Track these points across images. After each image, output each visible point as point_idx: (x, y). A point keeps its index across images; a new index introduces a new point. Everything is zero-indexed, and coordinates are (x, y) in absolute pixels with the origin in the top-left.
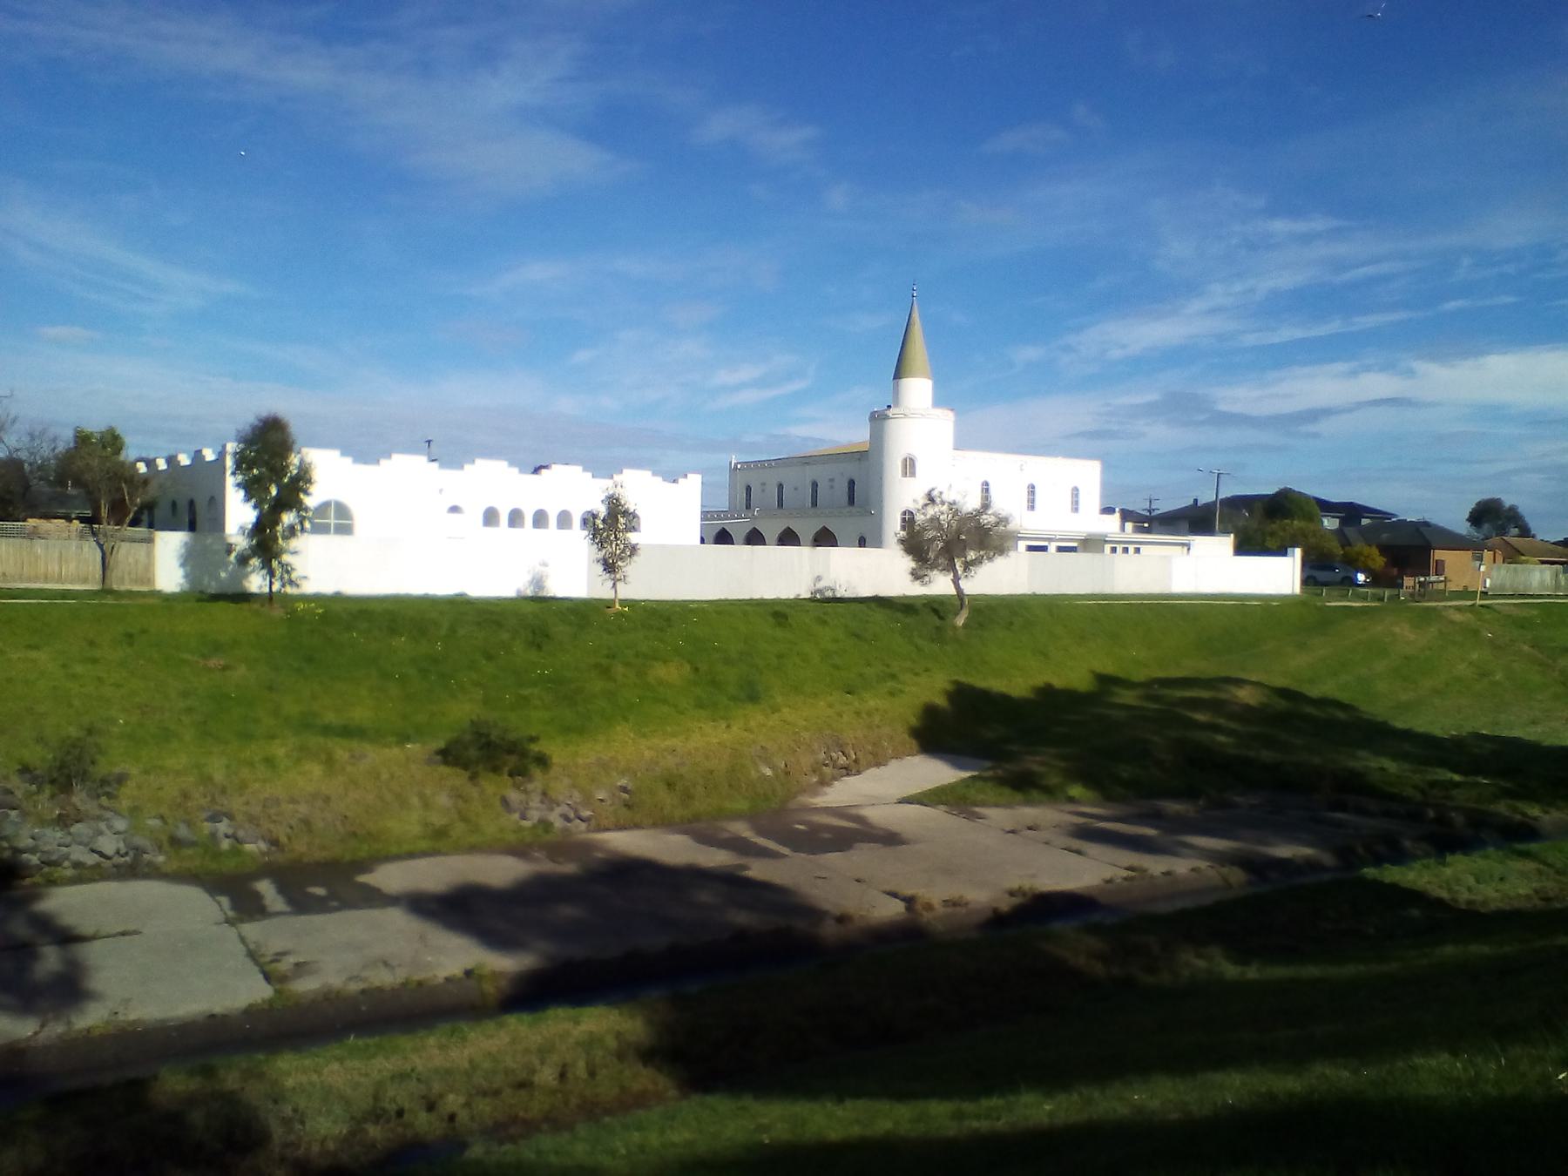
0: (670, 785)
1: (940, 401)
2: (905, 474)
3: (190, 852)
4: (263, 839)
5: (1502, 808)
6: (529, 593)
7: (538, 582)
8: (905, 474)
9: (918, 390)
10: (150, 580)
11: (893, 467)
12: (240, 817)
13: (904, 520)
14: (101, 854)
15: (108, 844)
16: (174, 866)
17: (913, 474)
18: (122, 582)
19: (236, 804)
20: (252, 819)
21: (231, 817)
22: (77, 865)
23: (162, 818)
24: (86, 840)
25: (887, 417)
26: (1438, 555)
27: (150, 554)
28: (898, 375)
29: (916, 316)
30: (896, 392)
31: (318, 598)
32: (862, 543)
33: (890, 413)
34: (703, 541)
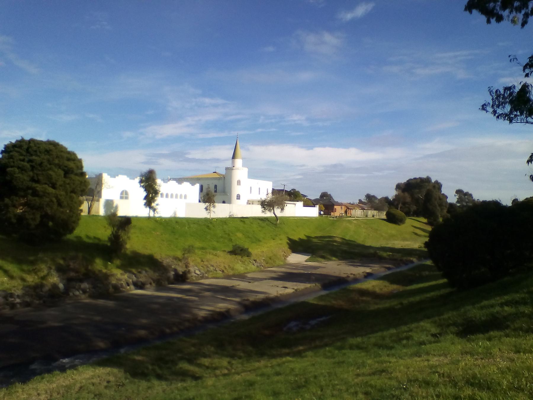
0: (270, 259)
2: (238, 185)
5: (405, 258)
6: (173, 216)
7: (175, 213)
8: (238, 185)
9: (239, 162)
10: (98, 212)
11: (235, 183)
14: (198, 274)
15: (198, 272)
16: (210, 276)
17: (240, 185)
18: (93, 212)
20: (217, 266)
21: (213, 266)
22: (195, 277)
25: (233, 169)
26: (335, 207)
27: (99, 205)
29: (238, 142)
30: (233, 163)
31: (161, 218)
32: (224, 202)
33: (234, 168)
34: (200, 202)
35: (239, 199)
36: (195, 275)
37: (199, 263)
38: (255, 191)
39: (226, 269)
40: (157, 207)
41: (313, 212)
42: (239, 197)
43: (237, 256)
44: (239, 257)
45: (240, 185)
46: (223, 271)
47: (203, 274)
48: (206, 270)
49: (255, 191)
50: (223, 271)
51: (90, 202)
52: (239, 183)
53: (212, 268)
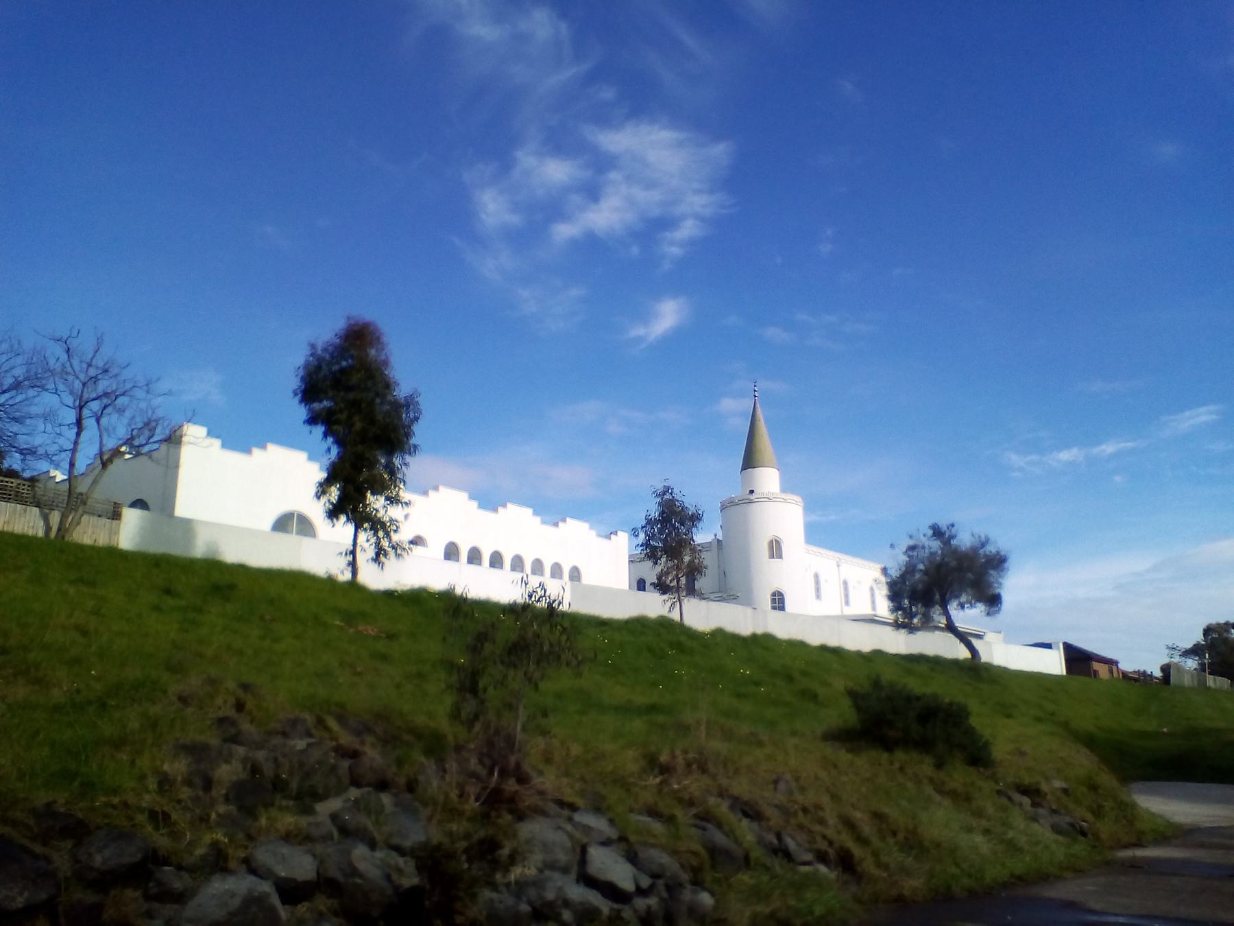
1: (788, 486)
2: (772, 556)
3: (745, 878)
4: (822, 857)
8: (772, 556)
9: (768, 479)
12: (769, 812)
13: (773, 601)
14: (610, 890)
17: (780, 557)
19: (741, 787)
21: (751, 812)
23: (653, 812)
24: (562, 857)
25: (751, 502)
28: (750, 461)
33: (753, 497)
35: (782, 608)
36: (577, 893)
37: (622, 782)
38: (832, 591)
39: (863, 841)
40: (395, 512)
41: (1053, 663)
42: (782, 601)
43: (900, 755)
44: (925, 766)
45: (780, 557)
46: (846, 862)
47: (673, 888)
48: (692, 840)
49: (832, 591)
50: (846, 862)
51: (55, 517)
52: (775, 549)
53: (747, 832)
